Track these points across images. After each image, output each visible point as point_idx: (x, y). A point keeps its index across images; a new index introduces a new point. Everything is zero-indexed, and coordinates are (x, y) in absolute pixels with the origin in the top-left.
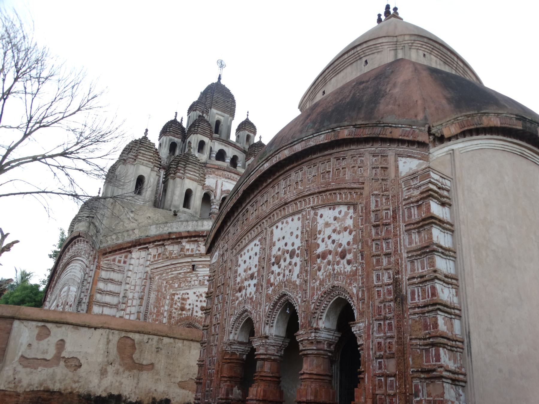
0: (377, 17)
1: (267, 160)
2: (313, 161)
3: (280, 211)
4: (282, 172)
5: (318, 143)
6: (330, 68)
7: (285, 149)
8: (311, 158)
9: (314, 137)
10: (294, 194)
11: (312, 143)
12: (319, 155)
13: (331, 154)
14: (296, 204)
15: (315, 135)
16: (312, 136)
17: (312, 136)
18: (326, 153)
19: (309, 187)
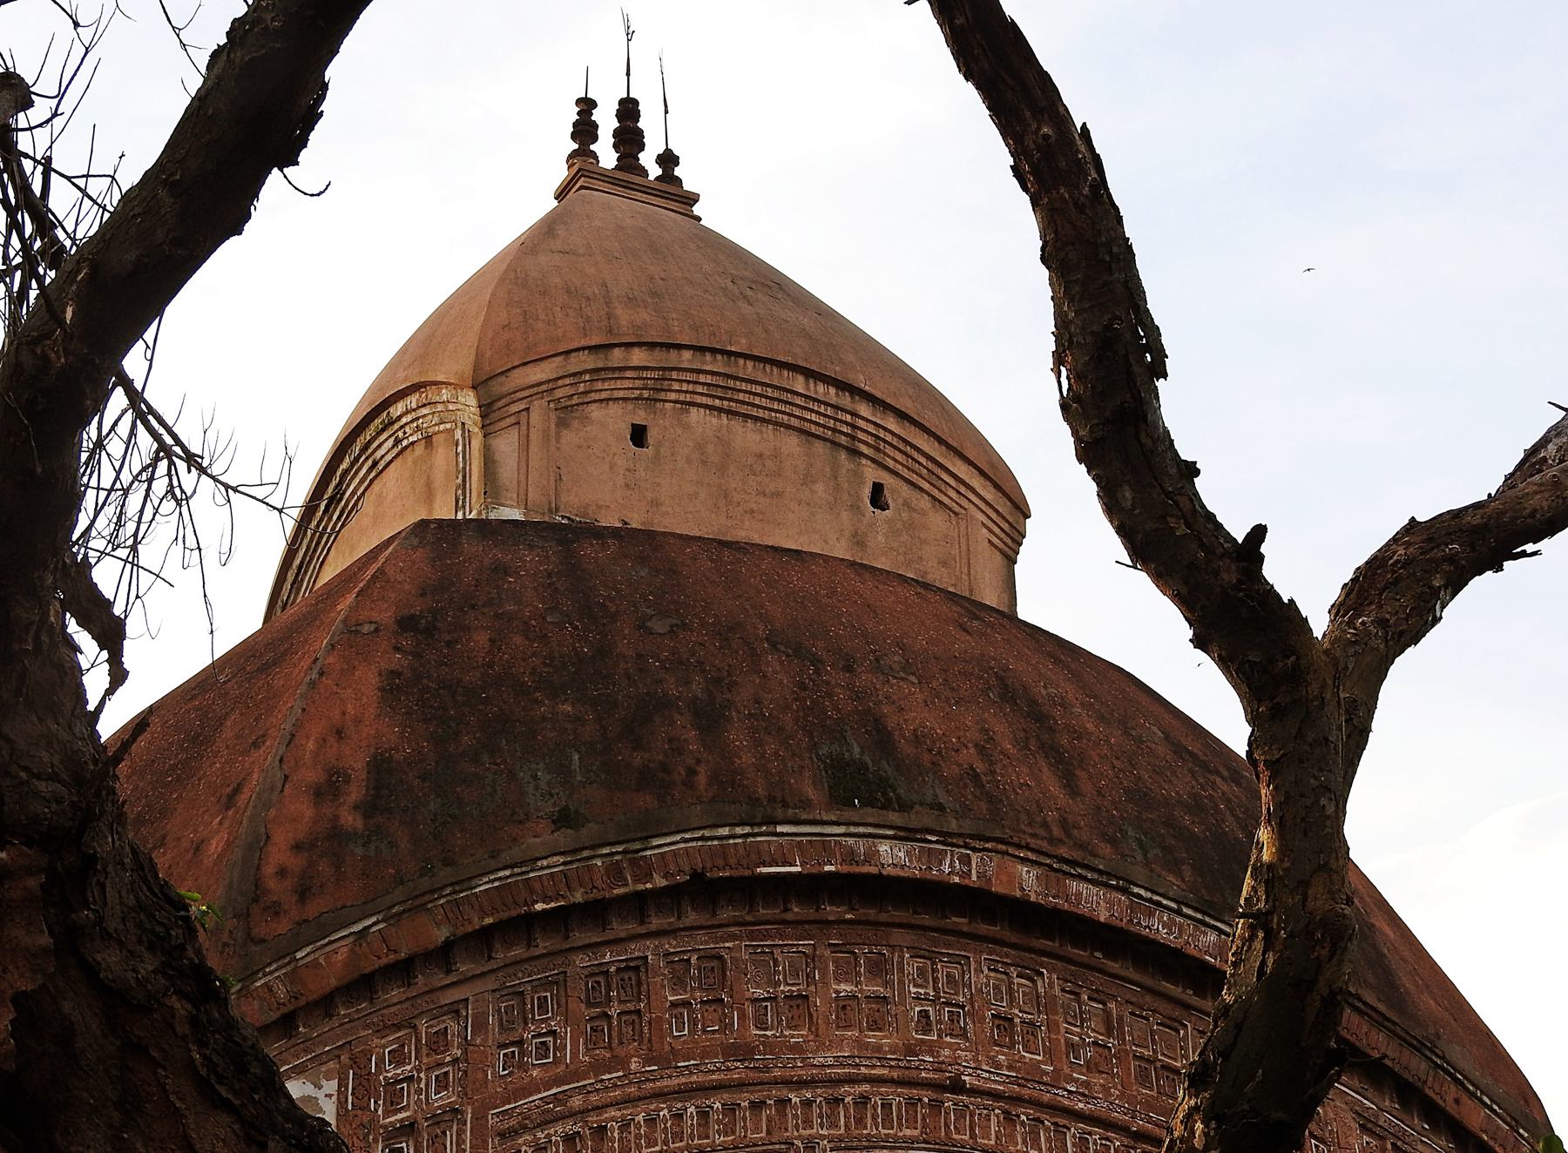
0: (572, 114)
1: (906, 834)
2: (1097, 980)
3: (912, 1103)
4: (926, 920)
5: (1191, 951)
6: (709, 363)
7: (1024, 860)
8: (1093, 962)
9: (1179, 912)
10: (998, 1066)
11: (1159, 928)
12: (1131, 974)
13: (1187, 1007)
14: (1009, 1118)
15: (1185, 910)
16: (1174, 905)
17: (1174, 905)
18: (1168, 987)
19: (1087, 1084)
